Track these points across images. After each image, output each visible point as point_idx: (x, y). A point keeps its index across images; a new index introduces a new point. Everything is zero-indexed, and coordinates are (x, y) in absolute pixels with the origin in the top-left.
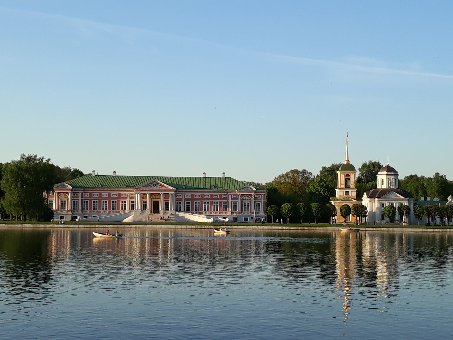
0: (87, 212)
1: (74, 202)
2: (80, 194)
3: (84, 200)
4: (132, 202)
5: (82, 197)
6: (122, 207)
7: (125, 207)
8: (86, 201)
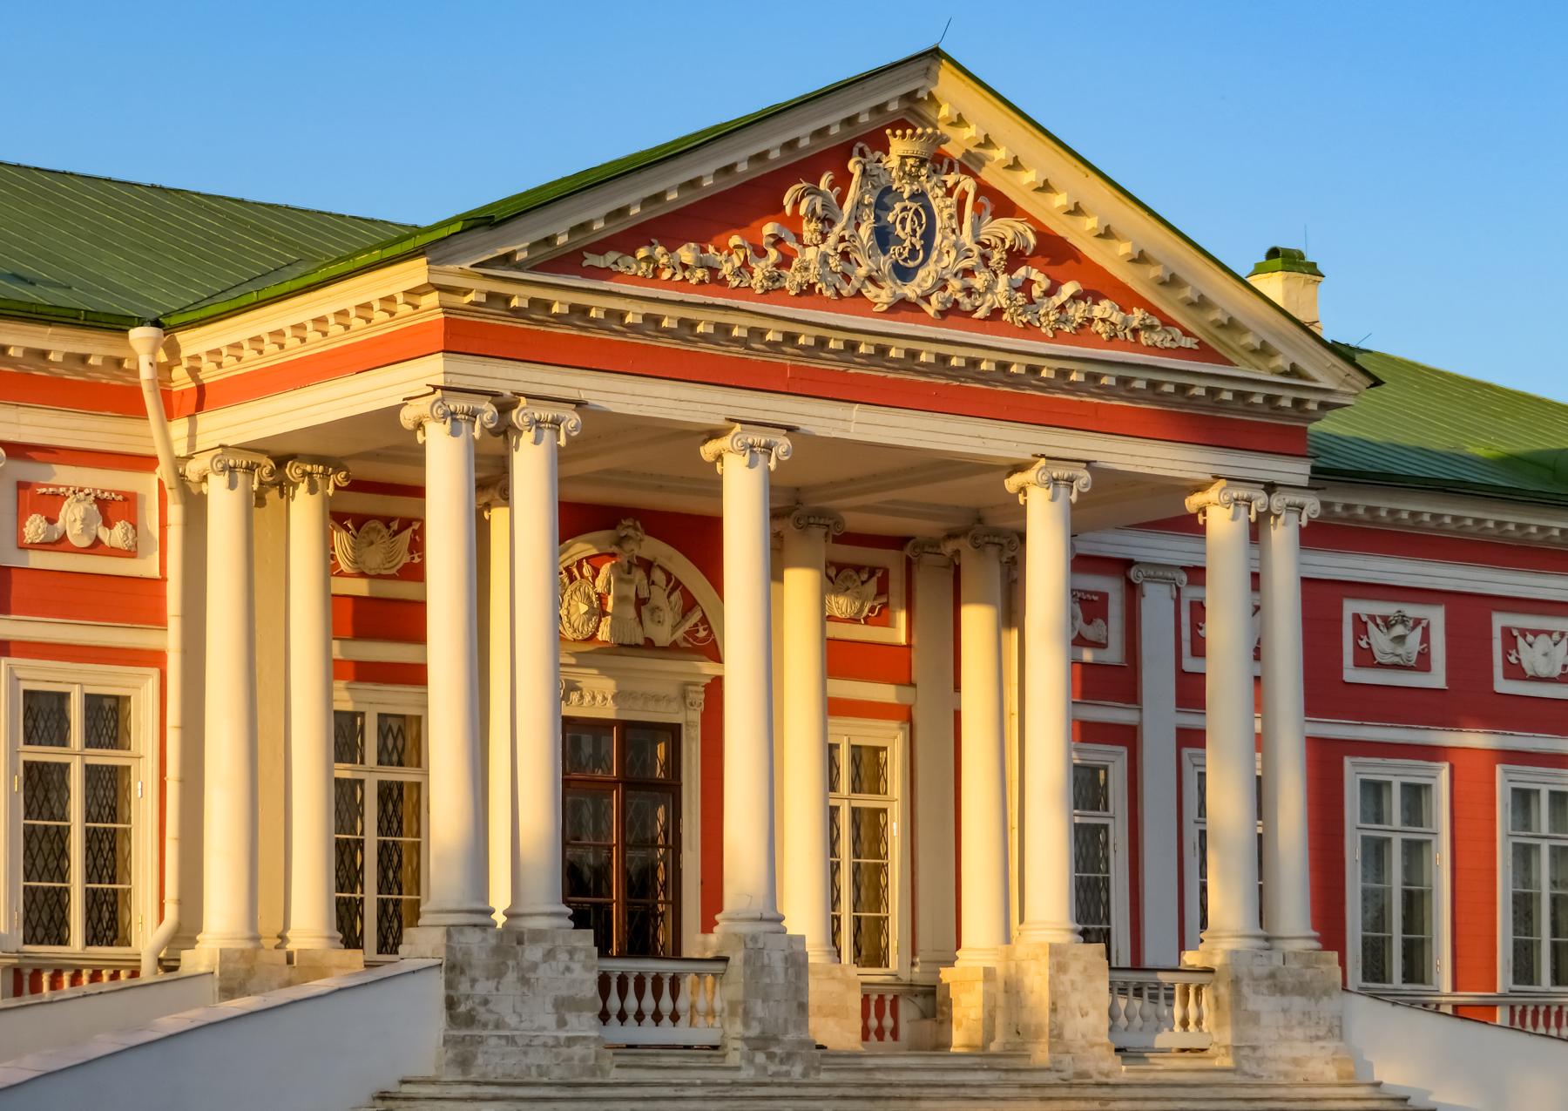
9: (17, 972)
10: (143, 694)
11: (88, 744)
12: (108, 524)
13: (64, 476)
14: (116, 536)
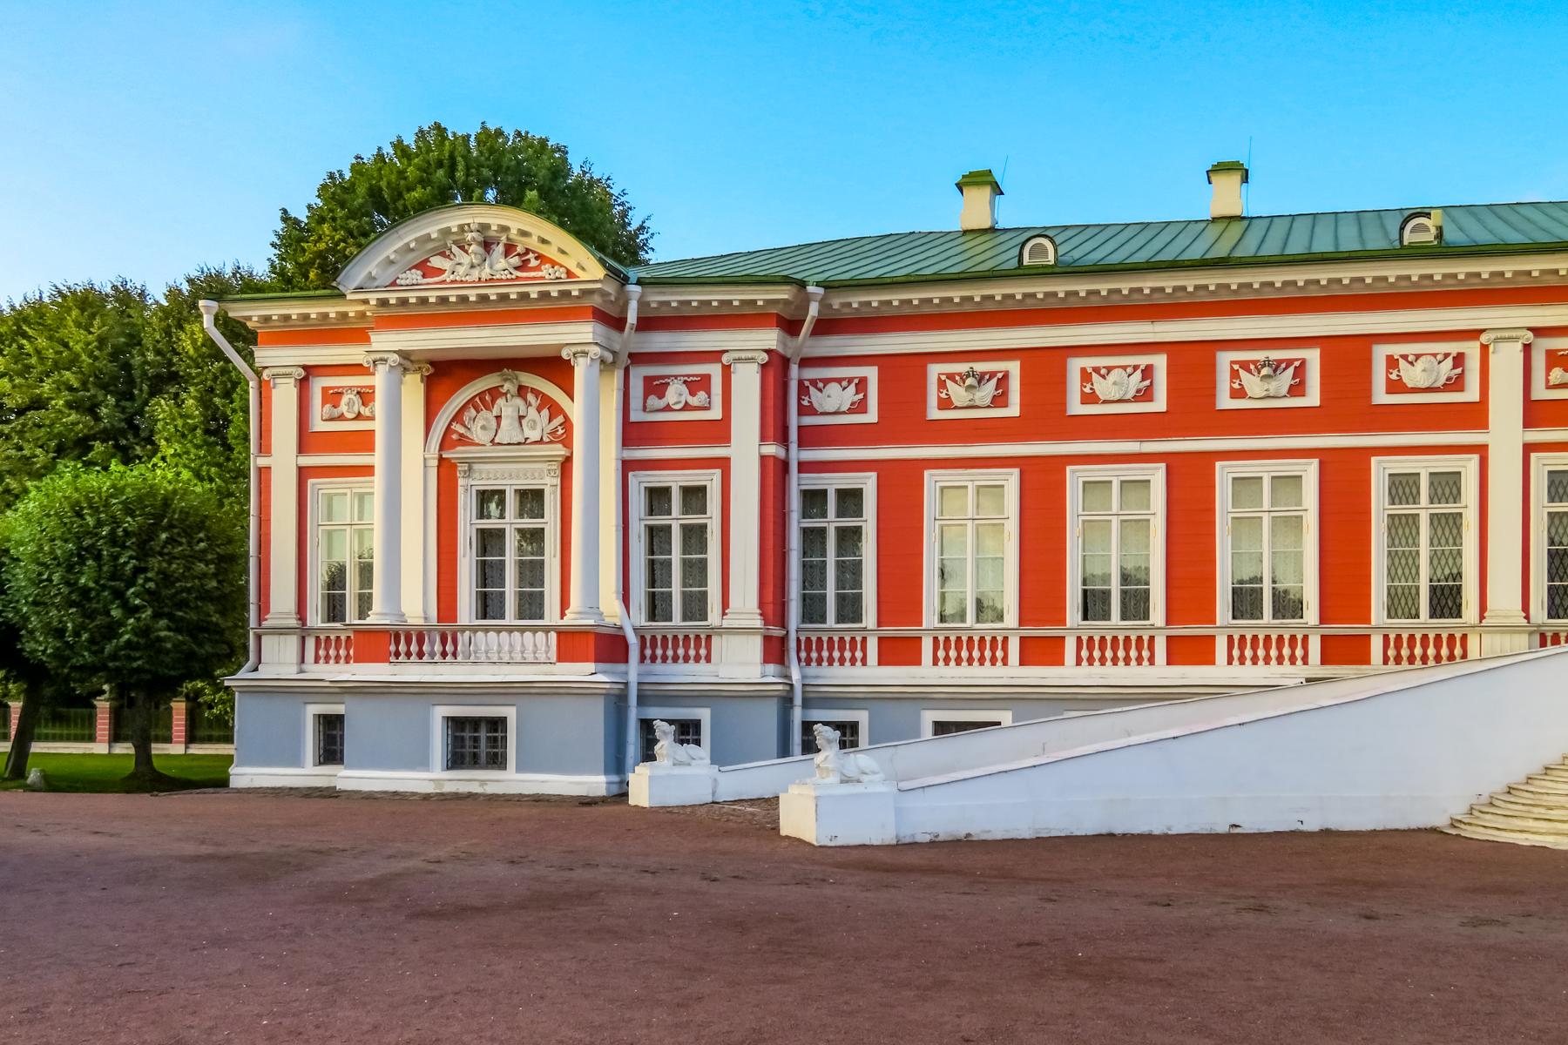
0: (850, 651)
1: (658, 498)
3: (797, 483)
5: (775, 426)
8: (833, 482)
9: (1543, 637)
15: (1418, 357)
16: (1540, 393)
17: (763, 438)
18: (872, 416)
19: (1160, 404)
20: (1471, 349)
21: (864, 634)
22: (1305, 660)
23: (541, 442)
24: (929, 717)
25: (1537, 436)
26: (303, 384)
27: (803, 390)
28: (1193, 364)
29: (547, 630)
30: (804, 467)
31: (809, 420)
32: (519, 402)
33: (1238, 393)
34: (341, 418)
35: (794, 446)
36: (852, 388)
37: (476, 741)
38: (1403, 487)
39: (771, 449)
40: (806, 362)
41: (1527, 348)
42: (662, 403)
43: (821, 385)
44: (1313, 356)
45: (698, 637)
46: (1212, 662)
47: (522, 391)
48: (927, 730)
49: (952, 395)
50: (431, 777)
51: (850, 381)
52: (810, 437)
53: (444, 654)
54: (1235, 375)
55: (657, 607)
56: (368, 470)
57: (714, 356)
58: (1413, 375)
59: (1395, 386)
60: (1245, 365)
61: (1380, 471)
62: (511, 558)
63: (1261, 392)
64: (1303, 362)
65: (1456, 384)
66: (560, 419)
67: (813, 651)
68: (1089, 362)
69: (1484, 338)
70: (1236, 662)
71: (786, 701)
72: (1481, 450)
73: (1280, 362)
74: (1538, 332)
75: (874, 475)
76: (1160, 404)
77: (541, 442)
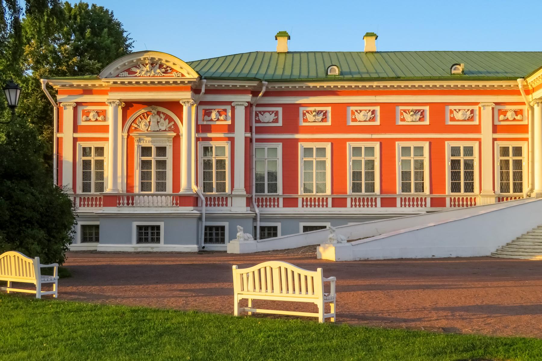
2: (240, 113)
4: (505, 151)
5: (249, 128)
6: (455, 175)
7: (469, 175)
10: (525, 146)
11: (513, 156)
12: (517, 115)
13: (508, 107)
14: (519, 117)
15: (459, 110)
16: (496, 123)
17: (246, 131)
18: (280, 124)
19: (378, 123)
20: (476, 108)
21: (278, 197)
22: (425, 205)
23: (165, 130)
24: (302, 224)
25: (496, 136)
26: (75, 109)
27: (257, 115)
28: (389, 110)
29: (166, 195)
30: (258, 140)
31: (259, 125)
32: (158, 117)
33: (403, 120)
34: (90, 120)
35: (254, 134)
36: (273, 114)
37: (149, 233)
38: (455, 151)
39: (249, 135)
40: (258, 105)
41: (493, 109)
42: (210, 118)
43: (262, 113)
44: (427, 108)
45: (222, 198)
46: (395, 206)
47: (159, 113)
48: (301, 229)
49: (310, 119)
50: (133, 246)
51: (273, 112)
52: (260, 130)
53: (128, 204)
54: (402, 114)
55: (207, 187)
56: (107, 139)
57: (229, 103)
58: (459, 116)
59: (453, 119)
60: (405, 111)
61: (448, 145)
62: (153, 170)
63: (409, 119)
64: (424, 111)
65: (471, 119)
66: (173, 123)
67: (261, 202)
68: (353, 108)
69: (480, 105)
70: (403, 206)
71: (255, 219)
72: (479, 140)
73: (416, 110)
74: (497, 104)
75: (281, 144)
76: (378, 123)
77: (165, 130)
